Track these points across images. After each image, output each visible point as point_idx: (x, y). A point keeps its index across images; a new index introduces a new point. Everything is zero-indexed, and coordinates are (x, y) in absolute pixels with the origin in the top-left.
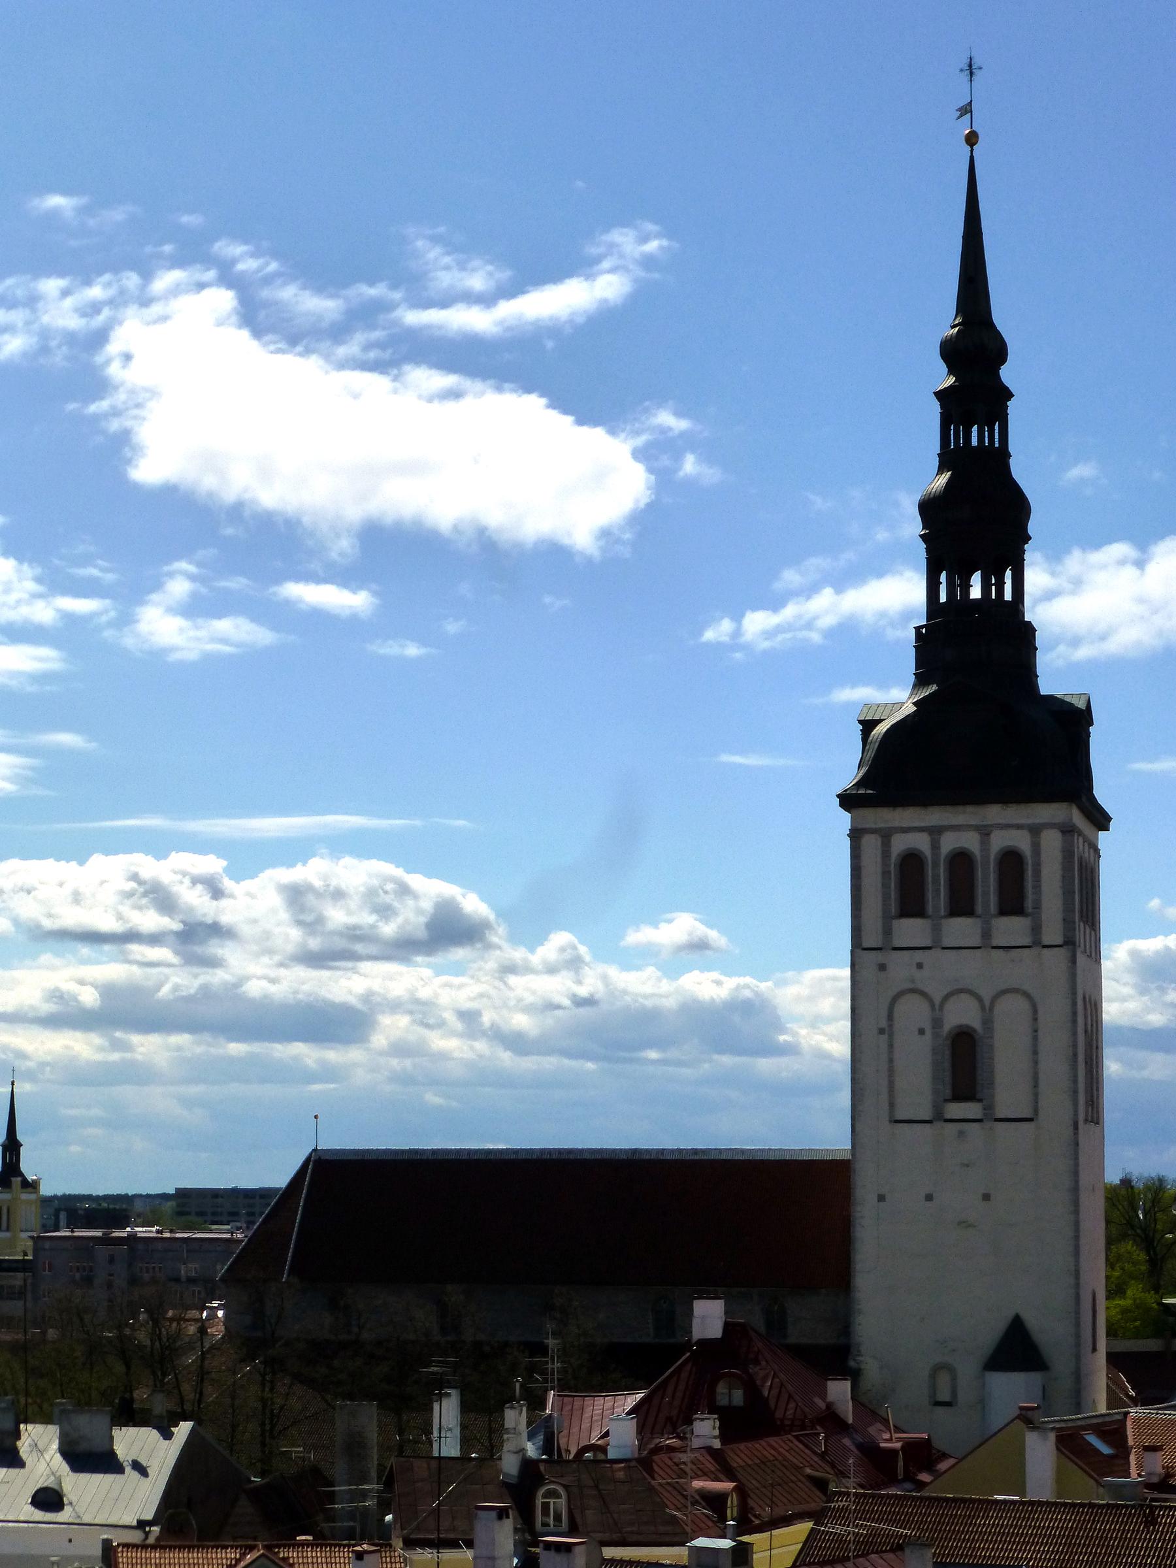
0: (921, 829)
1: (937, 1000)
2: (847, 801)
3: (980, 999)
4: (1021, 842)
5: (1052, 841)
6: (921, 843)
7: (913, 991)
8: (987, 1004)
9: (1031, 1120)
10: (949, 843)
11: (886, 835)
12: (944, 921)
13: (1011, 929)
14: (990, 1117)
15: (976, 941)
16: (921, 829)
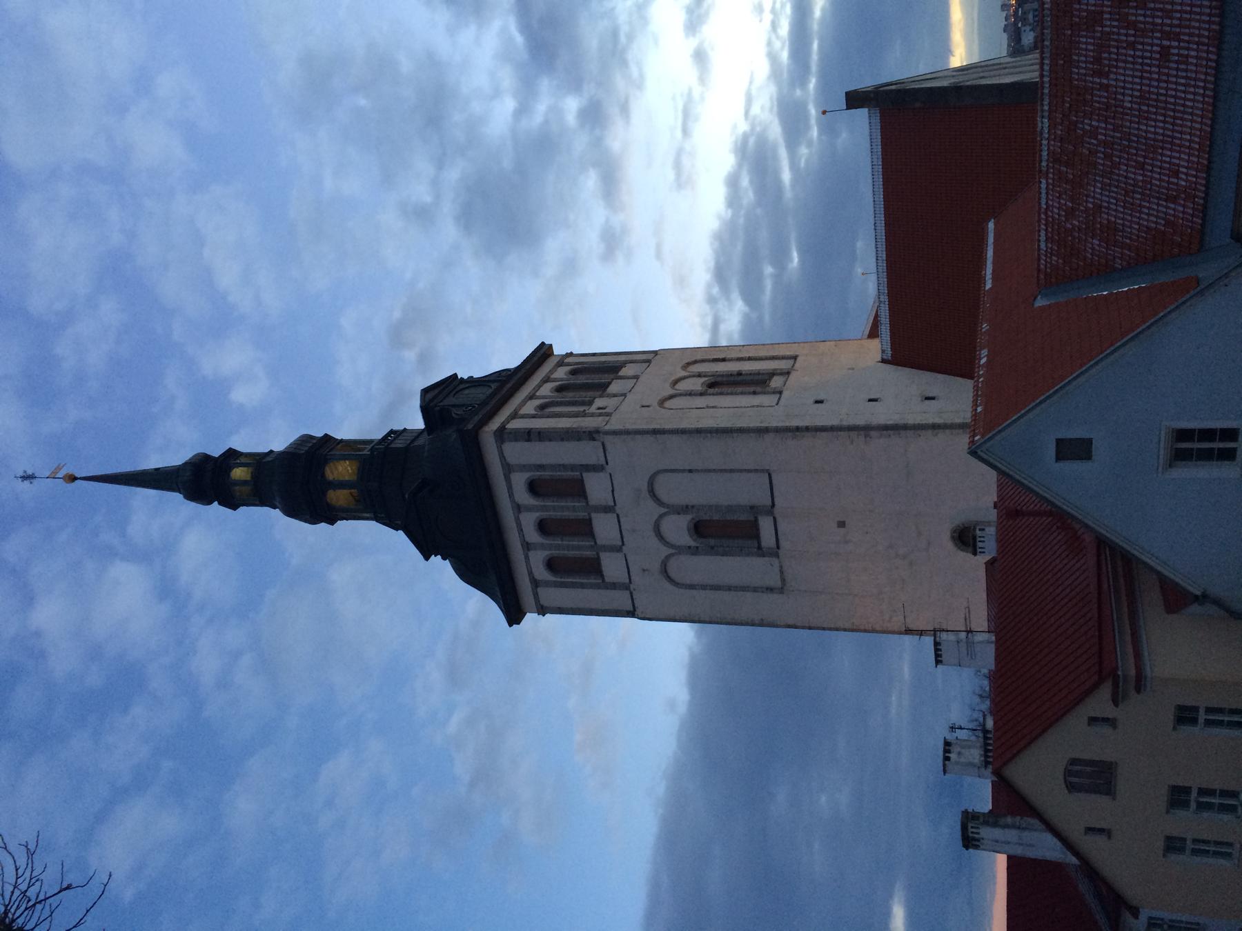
0: (527, 558)
1: (666, 551)
2: (514, 615)
3: (661, 516)
4: (520, 480)
5: (517, 452)
6: (538, 559)
7: (665, 571)
8: (663, 510)
9: (770, 475)
10: (533, 536)
11: (536, 583)
12: (599, 542)
13: (596, 487)
14: (770, 510)
15: (611, 518)
16: (527, 558)
